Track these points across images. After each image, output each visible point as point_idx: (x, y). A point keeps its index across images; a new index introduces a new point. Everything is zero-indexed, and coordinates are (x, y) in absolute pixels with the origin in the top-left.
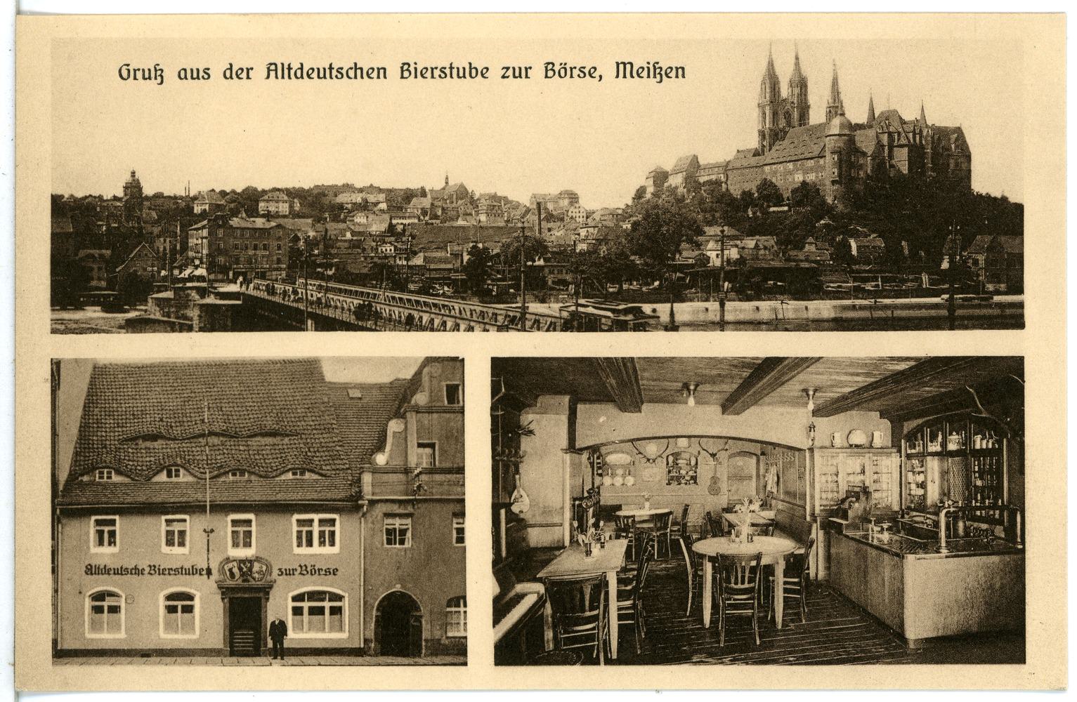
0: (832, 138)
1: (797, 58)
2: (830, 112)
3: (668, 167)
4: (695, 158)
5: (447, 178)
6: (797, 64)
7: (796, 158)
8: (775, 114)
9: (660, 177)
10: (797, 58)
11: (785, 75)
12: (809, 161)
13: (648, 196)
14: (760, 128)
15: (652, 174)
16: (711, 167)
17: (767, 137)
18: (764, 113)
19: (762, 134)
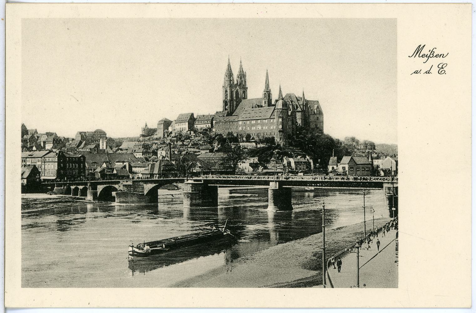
0: (278, 110)
1: (241, 62)
2: (265, 93)
3: (172, 117)
4: (192, 114)
6: (241, 66)
8: (232, 92)
9: (167, 124)
10: (241, 62)
11: (236, 73)
12: (264, 121)
13: (160, 134)
15: (163, 122)
18: (226, 91)
19: (225, 103)
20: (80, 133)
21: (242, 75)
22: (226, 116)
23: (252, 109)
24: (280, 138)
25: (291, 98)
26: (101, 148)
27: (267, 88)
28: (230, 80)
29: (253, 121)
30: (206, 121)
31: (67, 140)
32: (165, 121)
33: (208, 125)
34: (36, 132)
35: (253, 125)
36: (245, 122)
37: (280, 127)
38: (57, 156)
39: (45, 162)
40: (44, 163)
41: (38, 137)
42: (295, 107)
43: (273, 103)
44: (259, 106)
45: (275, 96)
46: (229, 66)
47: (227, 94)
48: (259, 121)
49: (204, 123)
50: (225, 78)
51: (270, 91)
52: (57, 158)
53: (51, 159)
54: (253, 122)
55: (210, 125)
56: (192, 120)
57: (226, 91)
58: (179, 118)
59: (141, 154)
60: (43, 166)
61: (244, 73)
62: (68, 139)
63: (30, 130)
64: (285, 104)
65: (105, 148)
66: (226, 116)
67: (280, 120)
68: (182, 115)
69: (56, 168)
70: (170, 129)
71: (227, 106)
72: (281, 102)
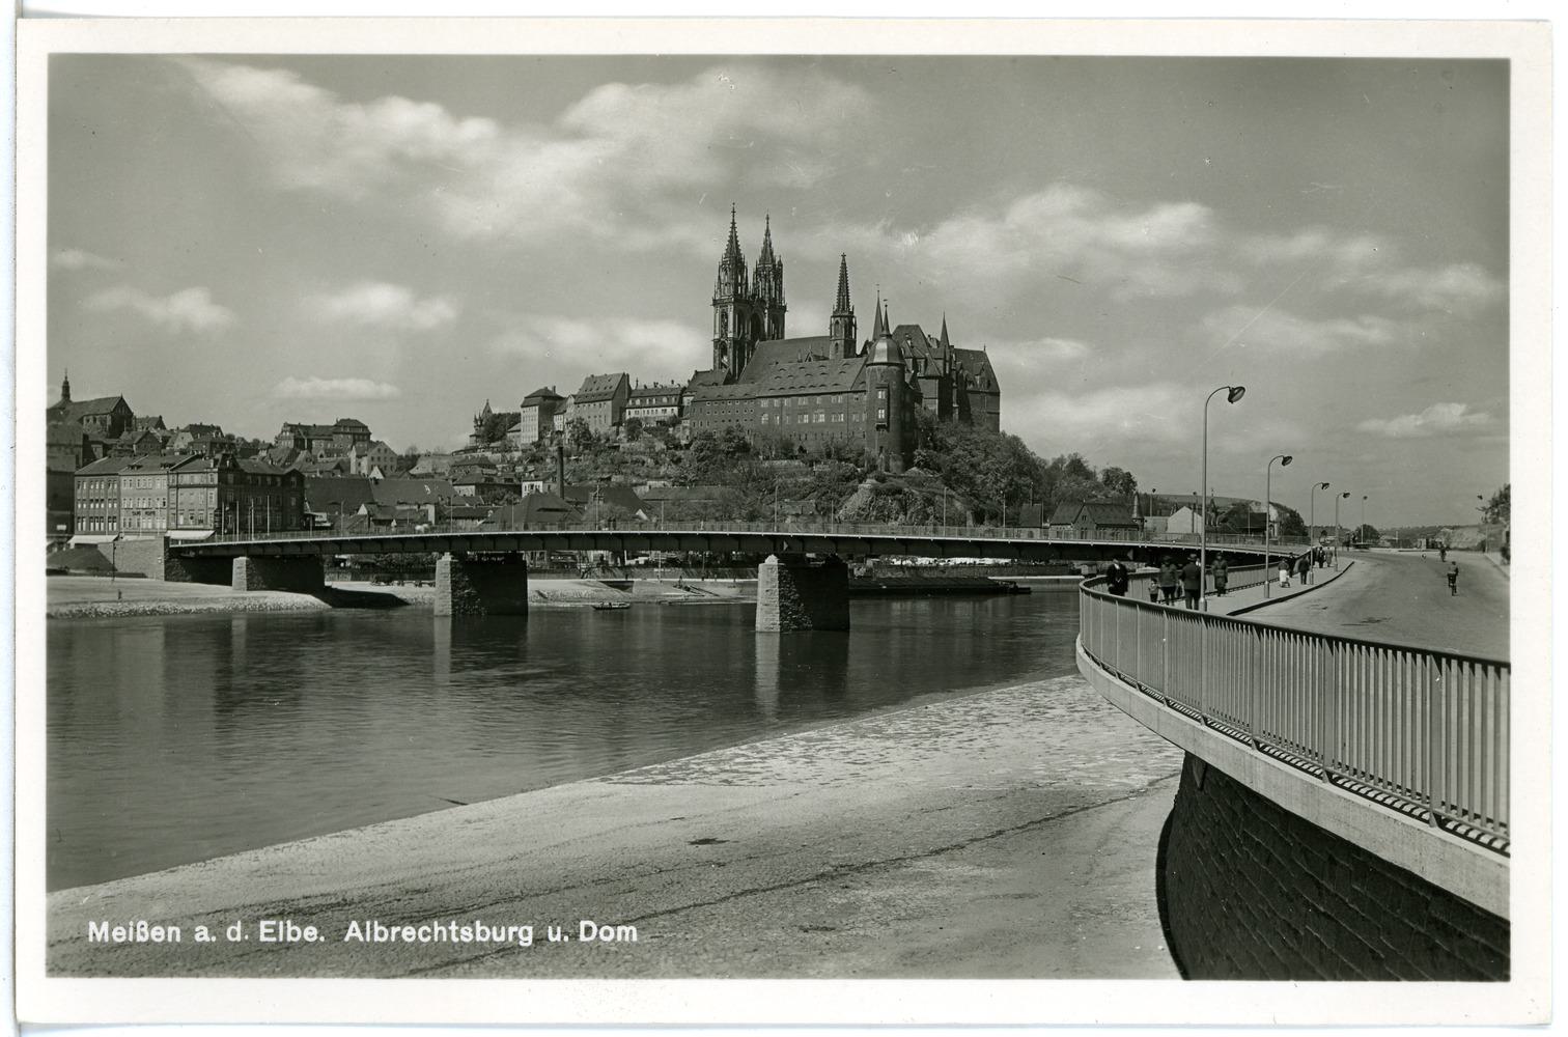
2: (837, 322)
5: (66, 387)
7: (812, 391)
8: (740, 315)
9: (549, 403)
12: (833, 398)
14: (717, 337)
16: (653, 395)
17: (730, 351)
18: (724, 316)
19: (721, 347)
20: (293, 428)
21: (772, 270)
22: (724, 384)
23: (801, 365)
24: (881, 448)
25: (909, 339)
26: (353, 470)
27: (843, 306)
28: (736, 285)
29: (800, 398)
30: (665, 400)
31: (252, 448)
32: (545, 398)
33: (669, 409)
34: (160, 423)
35: (803, 412)
36: (776, 401)
37: (882, 414)
38: (216, 470)
39: (178, 487)
40: (173, 492)
41: (166, 440)
42: (922, 365)
43: (858, 352)
44: (818, 358)
45: (864, 333)
46: (733, 241)
47: (726, 325)
48: (819, 398)
49: (659, 403)
50: (722, 278)
51: (851, 316)
52: (216, 476)
53: (197, 479)
54: (803, 402)
55: (676, 409)
56: (621, 393)
57: (722, 316)
58: (585, 388)
59: (473, 487)
60: (173, 500)
61: (777, 260)
62: (256, 442)
63: (142, 420)
64: (896, 352)
65: (365, 471)
66: (724, 384)
67: (881, 395)
68: (592, 379)
69: (214, 504)
70: (559, 422)
71: (725, 359)
72: (882, 346)
